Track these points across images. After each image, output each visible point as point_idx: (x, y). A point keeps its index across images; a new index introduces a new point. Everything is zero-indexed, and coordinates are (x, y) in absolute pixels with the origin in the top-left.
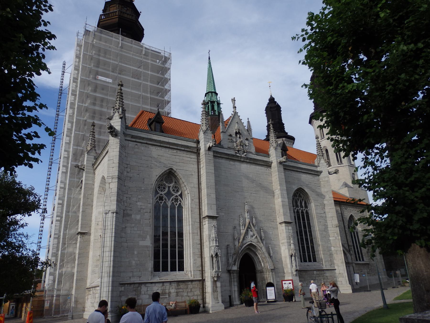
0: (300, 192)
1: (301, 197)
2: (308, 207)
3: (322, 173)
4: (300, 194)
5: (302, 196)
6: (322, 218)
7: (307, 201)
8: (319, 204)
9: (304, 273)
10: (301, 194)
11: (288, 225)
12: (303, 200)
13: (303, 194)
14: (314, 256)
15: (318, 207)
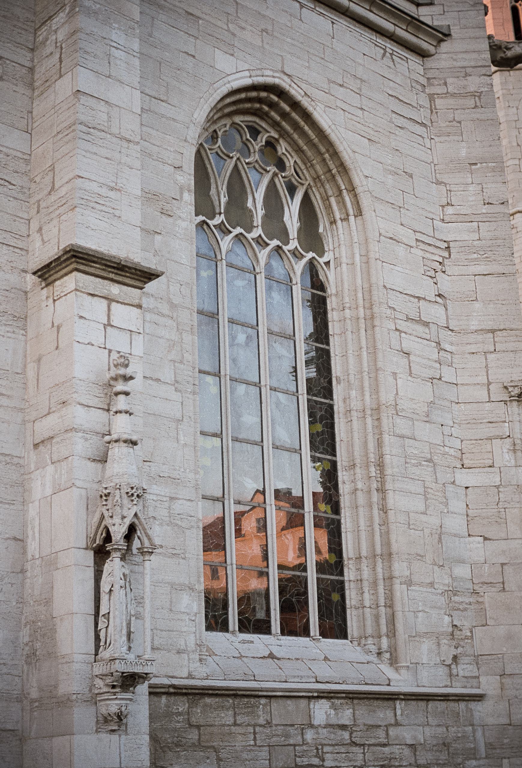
0: (276, 125)
1: (281, 165)
2: (329, 244)
3: (445, 47)
4: (271, 144)
5: (290, 162)
6: (420, 329)
7: (326, 199)
8: (408, 236)
9: (227, 717)
10: (283, 148)
11: (115, 290)
12: (292, 190)
13: (299, 151)
14: (335, 597)
15: (401, 250)
